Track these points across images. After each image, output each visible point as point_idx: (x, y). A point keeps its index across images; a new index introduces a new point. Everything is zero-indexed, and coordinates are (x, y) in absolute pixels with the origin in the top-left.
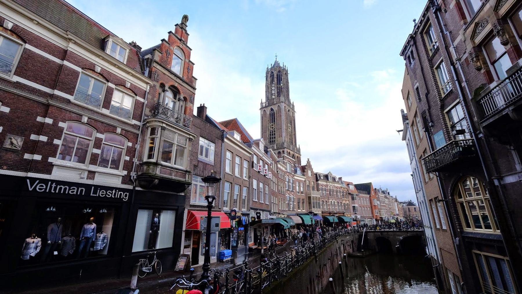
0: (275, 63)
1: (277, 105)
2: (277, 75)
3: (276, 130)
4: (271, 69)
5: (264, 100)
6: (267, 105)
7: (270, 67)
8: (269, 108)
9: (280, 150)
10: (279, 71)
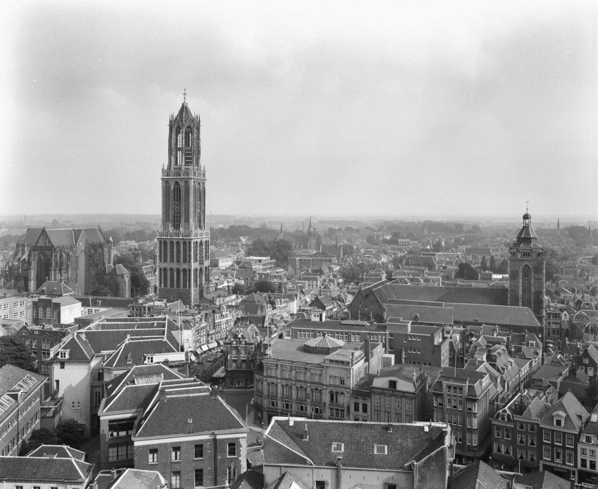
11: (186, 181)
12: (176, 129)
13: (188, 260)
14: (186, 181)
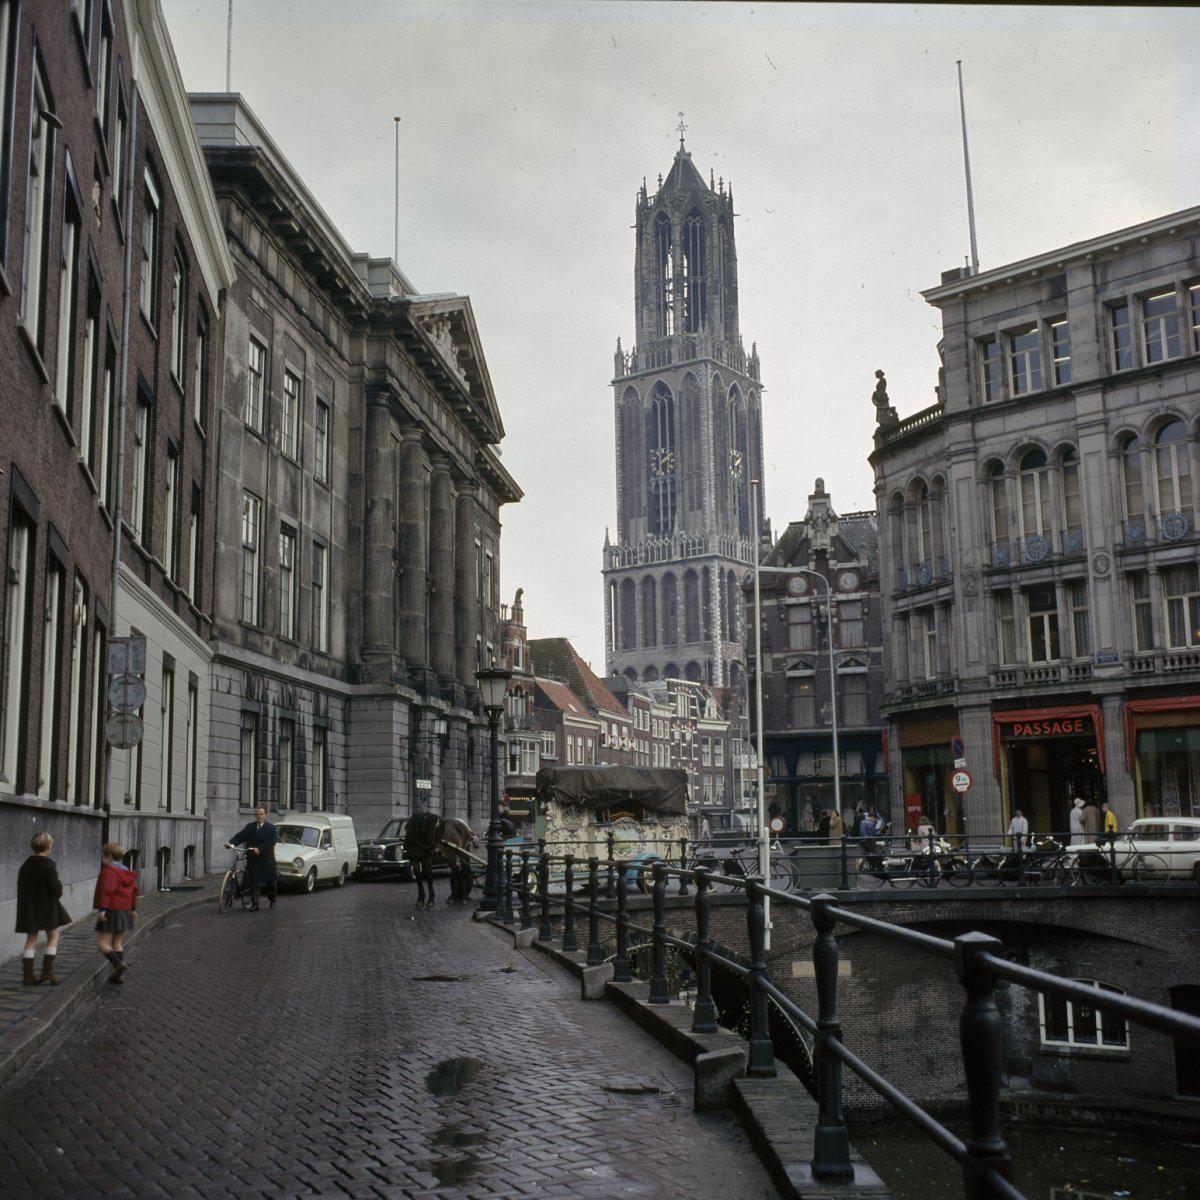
0: (677, 161)
1: (684, 372)
2: (685, 230)
3: (678, 478)
4: (660, 197)
5: (629, 345)
6: (642, 365)
7: (653, 191)
8: (653, 380)
9: (692, 565)
10: (695, 212)
11: (689, 374)
12: (656, 225)
13: (703, 630)
14: (689, 374)
